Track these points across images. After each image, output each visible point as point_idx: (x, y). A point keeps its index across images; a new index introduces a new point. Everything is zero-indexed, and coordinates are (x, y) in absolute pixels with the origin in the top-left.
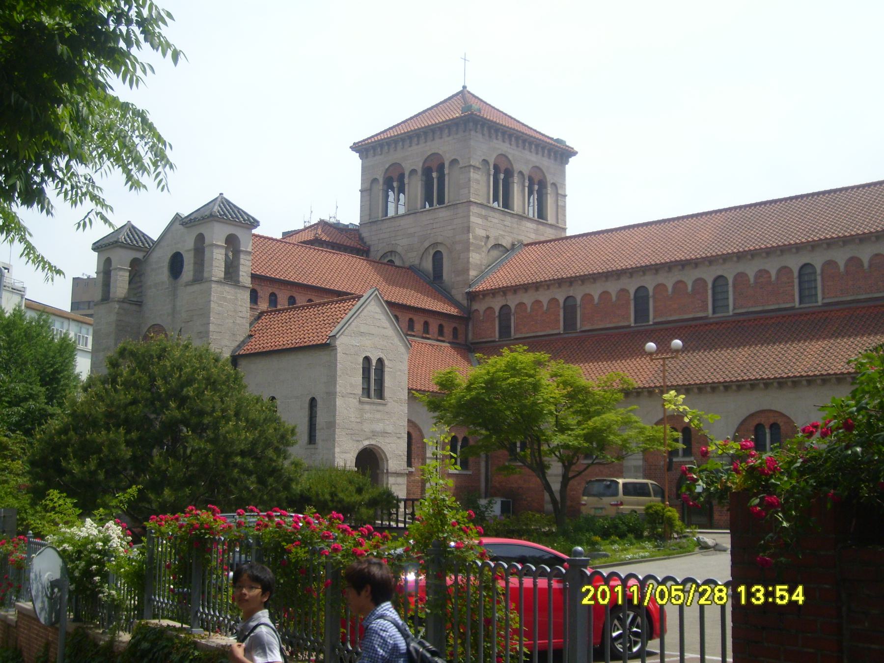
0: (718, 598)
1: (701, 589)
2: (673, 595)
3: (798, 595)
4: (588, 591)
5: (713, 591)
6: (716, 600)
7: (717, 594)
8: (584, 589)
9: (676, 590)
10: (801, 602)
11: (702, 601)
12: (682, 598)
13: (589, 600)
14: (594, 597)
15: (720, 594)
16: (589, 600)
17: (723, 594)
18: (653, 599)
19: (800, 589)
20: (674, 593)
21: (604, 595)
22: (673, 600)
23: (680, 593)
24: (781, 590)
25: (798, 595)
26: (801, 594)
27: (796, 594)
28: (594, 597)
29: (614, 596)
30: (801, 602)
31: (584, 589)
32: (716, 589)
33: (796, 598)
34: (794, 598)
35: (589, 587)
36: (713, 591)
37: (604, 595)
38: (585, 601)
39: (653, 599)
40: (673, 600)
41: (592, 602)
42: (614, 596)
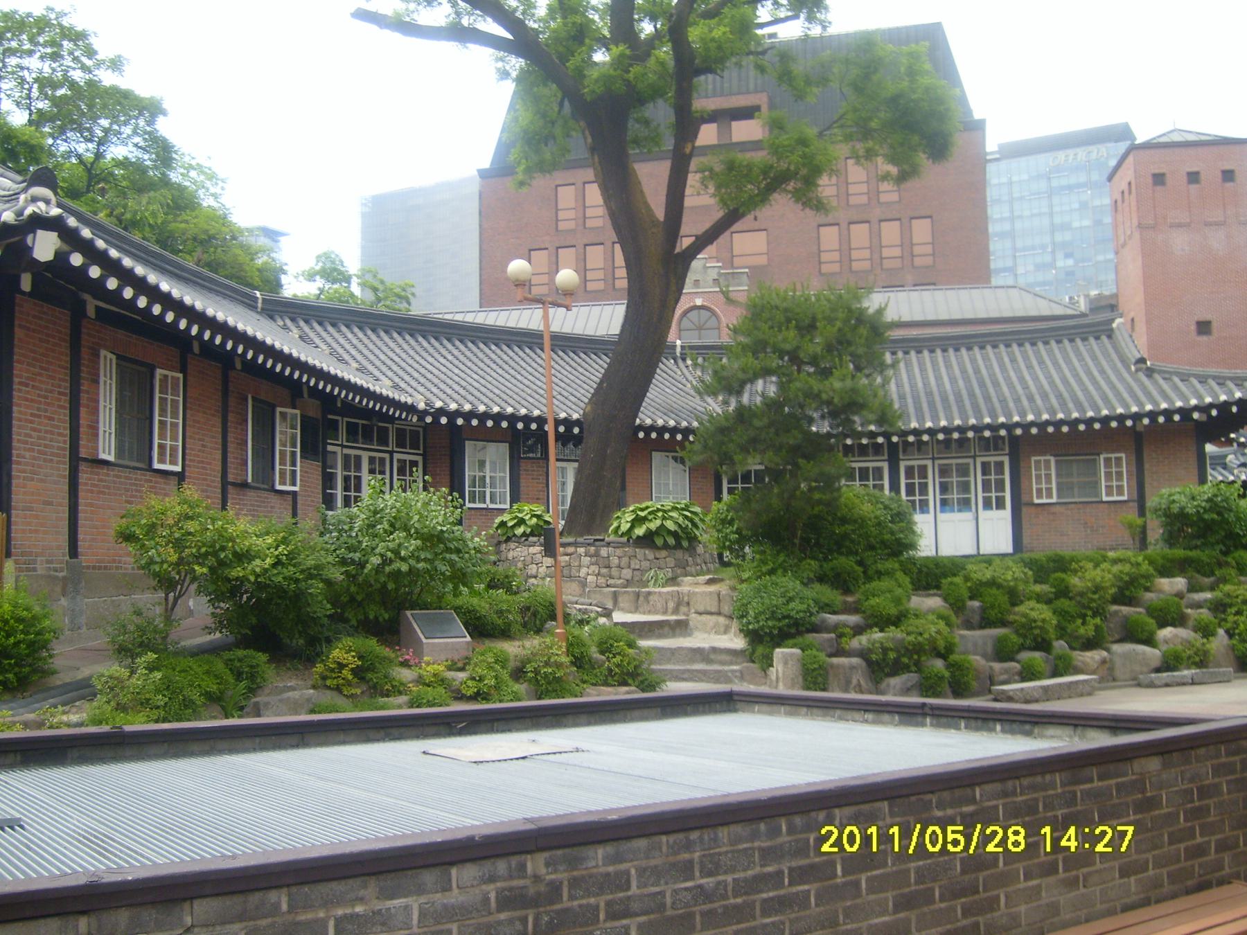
0: (1013, 844)
1: (988, 831)
2: (949, 840)
3: (1069, 840)
4: (830, 833)
5: (1005, 833)
6: (1010, 846)
7: (1012, 838)
8: (823, 831)
9: (953, 832)
10: (1073, 849)
11: (991, 848)
12: (962, 843)
13: (831, 846)
14: (838, 843)
15: (1016, 838)
16: (831, 846)
17: (1021, 838)
18: (921, 845)
19: (1072, 830)
20: (950, 837)
21: (851, 840)
22: (950, 847)
23: (959, 837)
24: (953, 832)
25: (1069, 840)
26: (1073, 838)
27: (1066, 837)
28: (838, 843)
29: (867, 840)
30: (1073, 849)
31: (823, 831)
32: (1010, 831)
33: (1068, 844)
34: (1064, 843)
35: (996, 828)
36: (1005, 833)
37: (851, 840)
38: (826, 848)
39: (921, 845)
40: (950, 847)
41: (836, 850)
42: (867, 840)
